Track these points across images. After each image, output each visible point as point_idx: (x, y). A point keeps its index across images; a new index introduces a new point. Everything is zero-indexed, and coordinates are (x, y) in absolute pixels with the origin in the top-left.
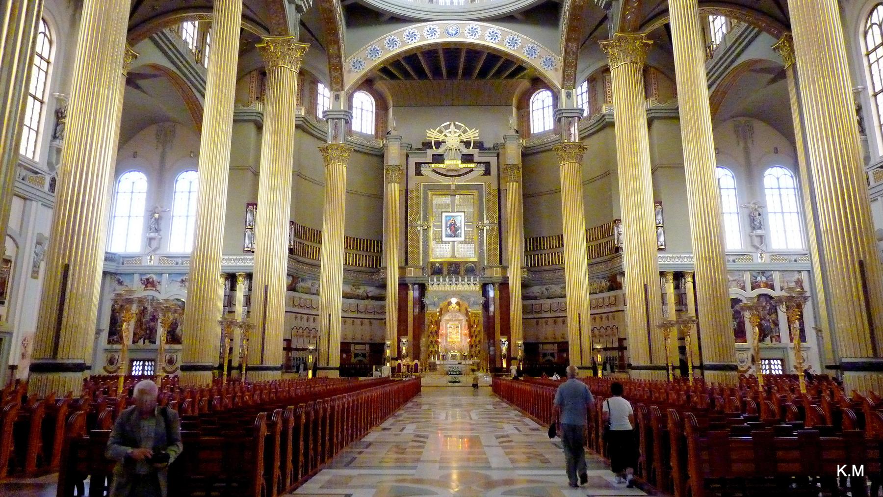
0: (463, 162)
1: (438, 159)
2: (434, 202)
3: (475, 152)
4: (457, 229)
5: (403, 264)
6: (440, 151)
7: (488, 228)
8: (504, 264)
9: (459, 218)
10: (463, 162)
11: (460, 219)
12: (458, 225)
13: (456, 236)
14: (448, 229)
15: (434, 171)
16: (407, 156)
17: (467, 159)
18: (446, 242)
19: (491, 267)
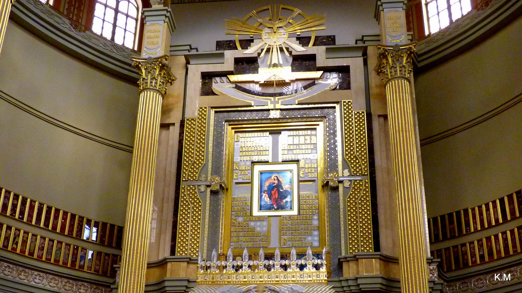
0: (293, 71)
1: (248, 64)
2: (237, 146)
3: (320, 52)
4: (282, 195)
5: (166, 253)
6: (251, 51)
7: (347, 184)
8: (386, 249)
9: (288, 175)
10: (293, 71)
11: (289, 178)
12: (286, 186)
13: (281, 208)
14: (266, 198)
15: (239, 86)
16: (188, 63)
17: (303, 62)
18: (260, 219)
19: (356, 259)
